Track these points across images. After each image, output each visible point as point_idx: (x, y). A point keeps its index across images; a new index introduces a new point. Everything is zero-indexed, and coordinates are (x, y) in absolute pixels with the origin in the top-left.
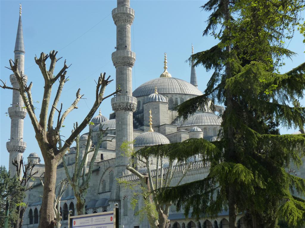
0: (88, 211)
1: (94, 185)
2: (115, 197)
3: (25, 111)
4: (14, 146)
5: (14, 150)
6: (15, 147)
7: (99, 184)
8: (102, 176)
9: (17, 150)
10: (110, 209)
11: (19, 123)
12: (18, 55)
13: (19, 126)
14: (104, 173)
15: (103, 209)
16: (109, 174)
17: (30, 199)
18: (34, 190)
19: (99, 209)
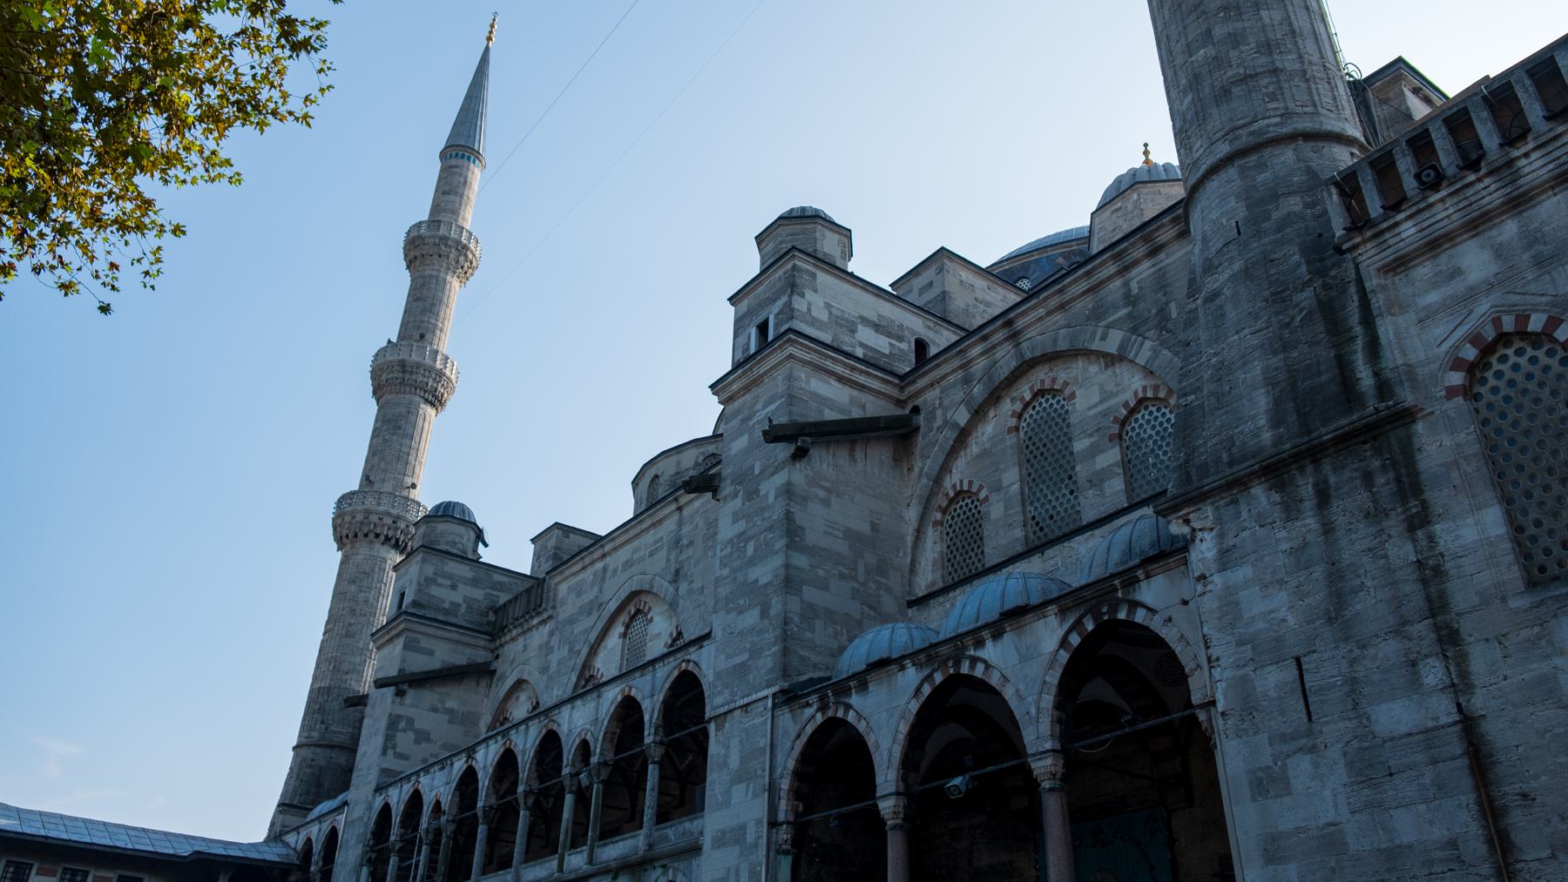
4: (368, 513)
7: (919, 532)
8: (945, 468)
9: (377, 536)
15: (1077, 626)
16: (1017, 429)
17: (394, 747)
18: (428, 696)
19: (1008, 638)
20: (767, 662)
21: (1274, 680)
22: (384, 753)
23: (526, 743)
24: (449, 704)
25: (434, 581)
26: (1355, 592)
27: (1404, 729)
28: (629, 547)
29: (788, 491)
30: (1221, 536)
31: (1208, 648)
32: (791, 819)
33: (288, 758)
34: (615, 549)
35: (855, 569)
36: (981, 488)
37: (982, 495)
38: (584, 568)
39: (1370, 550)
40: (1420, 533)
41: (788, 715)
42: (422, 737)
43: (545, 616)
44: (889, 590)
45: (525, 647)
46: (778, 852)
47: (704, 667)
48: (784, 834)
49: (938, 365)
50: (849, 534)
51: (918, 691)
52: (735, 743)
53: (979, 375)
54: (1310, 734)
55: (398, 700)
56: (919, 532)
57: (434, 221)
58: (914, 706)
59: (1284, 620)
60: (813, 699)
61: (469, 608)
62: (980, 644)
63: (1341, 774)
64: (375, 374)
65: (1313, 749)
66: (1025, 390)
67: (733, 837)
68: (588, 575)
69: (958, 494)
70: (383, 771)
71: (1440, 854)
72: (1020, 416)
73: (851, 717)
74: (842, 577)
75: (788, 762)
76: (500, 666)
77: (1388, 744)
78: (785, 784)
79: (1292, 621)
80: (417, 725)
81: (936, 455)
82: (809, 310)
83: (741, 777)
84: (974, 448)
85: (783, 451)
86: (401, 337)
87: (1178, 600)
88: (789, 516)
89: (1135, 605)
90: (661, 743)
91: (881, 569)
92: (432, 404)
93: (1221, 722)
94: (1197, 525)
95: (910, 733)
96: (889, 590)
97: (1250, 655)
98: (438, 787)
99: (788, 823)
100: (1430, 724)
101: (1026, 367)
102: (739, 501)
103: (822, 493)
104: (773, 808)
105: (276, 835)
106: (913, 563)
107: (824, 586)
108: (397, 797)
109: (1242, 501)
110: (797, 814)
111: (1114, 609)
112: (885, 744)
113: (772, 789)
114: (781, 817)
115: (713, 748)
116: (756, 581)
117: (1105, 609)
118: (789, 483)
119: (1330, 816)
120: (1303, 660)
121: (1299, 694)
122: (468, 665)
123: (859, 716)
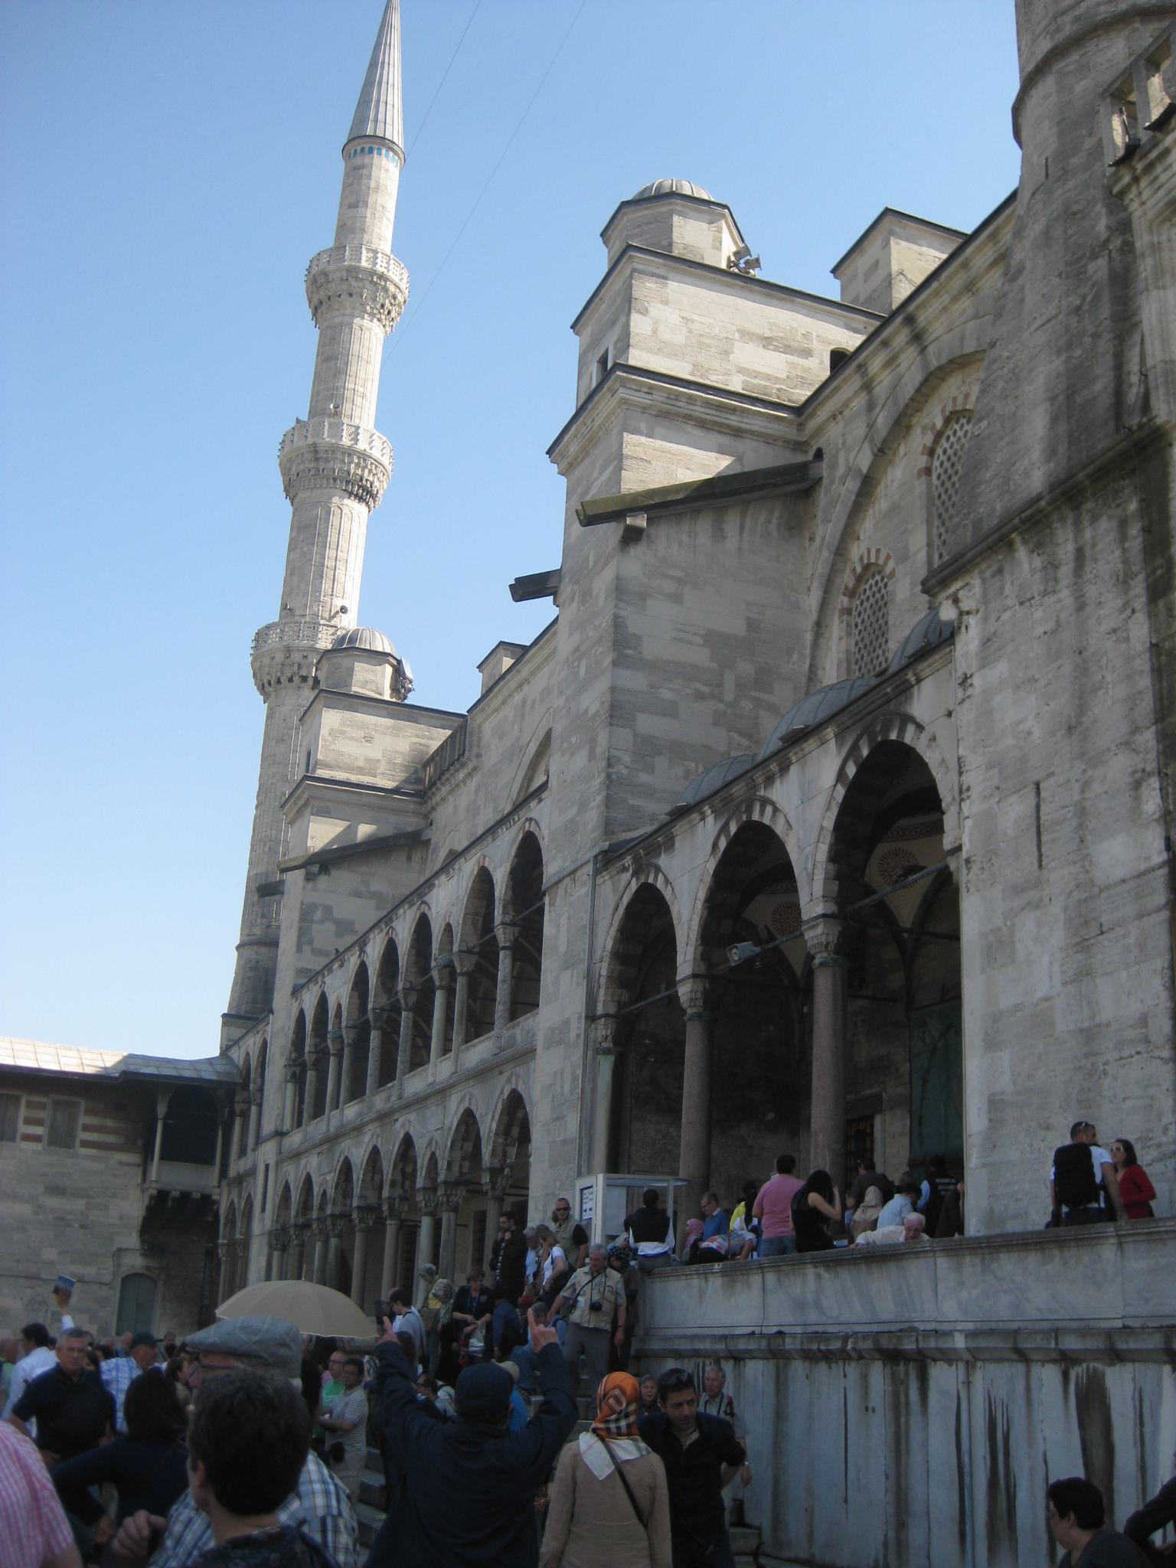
0: (663, 861)
1: (752, 625)
2: (1051, 452)
3: (376, 453)
4: (288, 650)
5: (291, 680)
6: (296, 657)
7: (819, 626)
8: (848, 533)
9: (304, 679)
10: (965, 681)
11: (334, 520)
12: (358, 160)
13: (332, 537)
14: (868, 485)
15: (855, 749)
17: (310, 942)
18: (344, 878)
19: (794, 770)
20: (593, 815)
21: (1015, 810)
22: (299, 949)
23: (404, 931)
24: (375, 886)
25: (343, 733)
26: (1094, 691)
27: (1119, 873)
28: (546, 669)
29: (619, 589)
30: (985, 619)
31: (961, 774)
32: (612, 1010)
33: (233, 956)
34: (534, 673)
35: (720, 685)
36: (888, 557)
37: (888, 570)
38: (504, 702)
39: (1114, 631)
40: (1161, 604)
41: (609, 883)
42: (344, 927)
43: (471, 766)
44: (773, 709)
45: (455, 807)
46: (597, 1051)
47: (543, 824)
48: (603, 1031)
49: (837, 389)
50: (714, 640)
51: (715, 846)
52: (563, 920)
53: (881, 401)
54: (1038, 883)
55: (310, 885)
56: (819, 626)
57: (339, 248)
58: (711, 866)
59: (1029, 733)
60: (628, 861)
61: (391, 762)
62: (769, 781)
63: (1058, 937)
64: (285, 468)
65: (1036, 905)
66: (934, 414)
67: (558, 1036)
68: (508, 712)
69: (867, 567)
70: (300, 972)
71: (1130, 1034)
72: (931, 452)
73: (660, 884)
74: (699, 696)
75: (606, 939)
76: (435, 835)
77: (1103, 895)
78: (604, 969)
79: (1037, 732)
80: (338, 914)
81: (839, 514)
82: (655, 332)
83: (568, 964)
84: (882, 502)
85: (611, 532)
86: (313, 413)
87: (942, 712)
88: (618, 623)
89: (908, 719)
90: (513, 924)
91: (763, 680)
92: (360, 499)
93: (964, 871)
94: (965, 605)
95: (706, 901)
96: (773, 709)
97: (996, 782)
98: (339, 988)
99: (606, 1016)
100: (1143, 866)
101: (932, 380)
102: (575, 604)
103: (669, 587)
104: (591, 1000)
105: (225, 1050)
106: (813, 669)
107: (670, 711)
108: (309, 1001)
109: (1007, 569)
110: (621, 1005)
111: (887, 729)
112: (685, 916)
113: (590, 976)
114: (600, 1010)
115: (548, 929)
116: (587, 711)
117: (878, 728)
118: (618, 578)
119: (1042, 991)
120: (1042, 786)
121: (1034, 830)
122: (395, 837)
123: (667, 881)
